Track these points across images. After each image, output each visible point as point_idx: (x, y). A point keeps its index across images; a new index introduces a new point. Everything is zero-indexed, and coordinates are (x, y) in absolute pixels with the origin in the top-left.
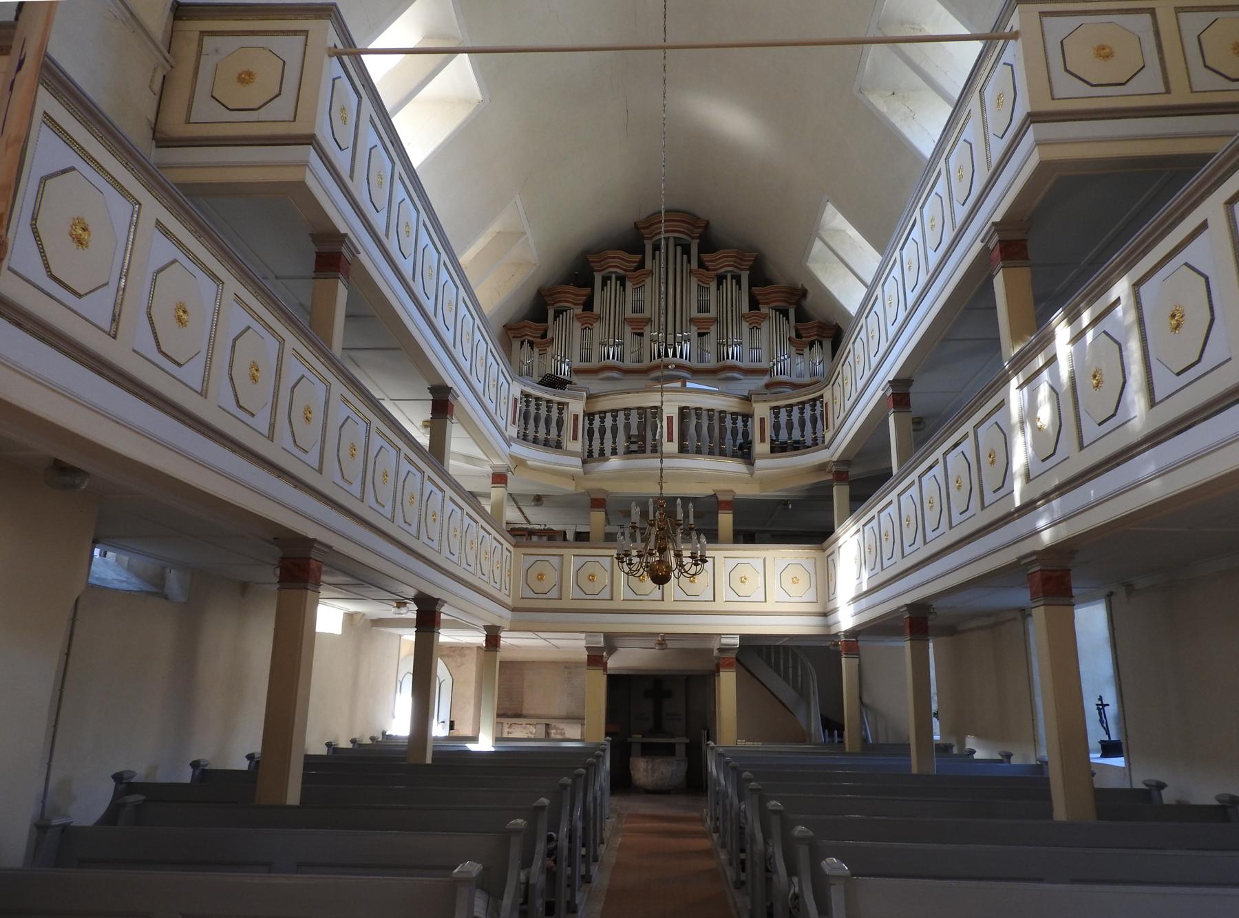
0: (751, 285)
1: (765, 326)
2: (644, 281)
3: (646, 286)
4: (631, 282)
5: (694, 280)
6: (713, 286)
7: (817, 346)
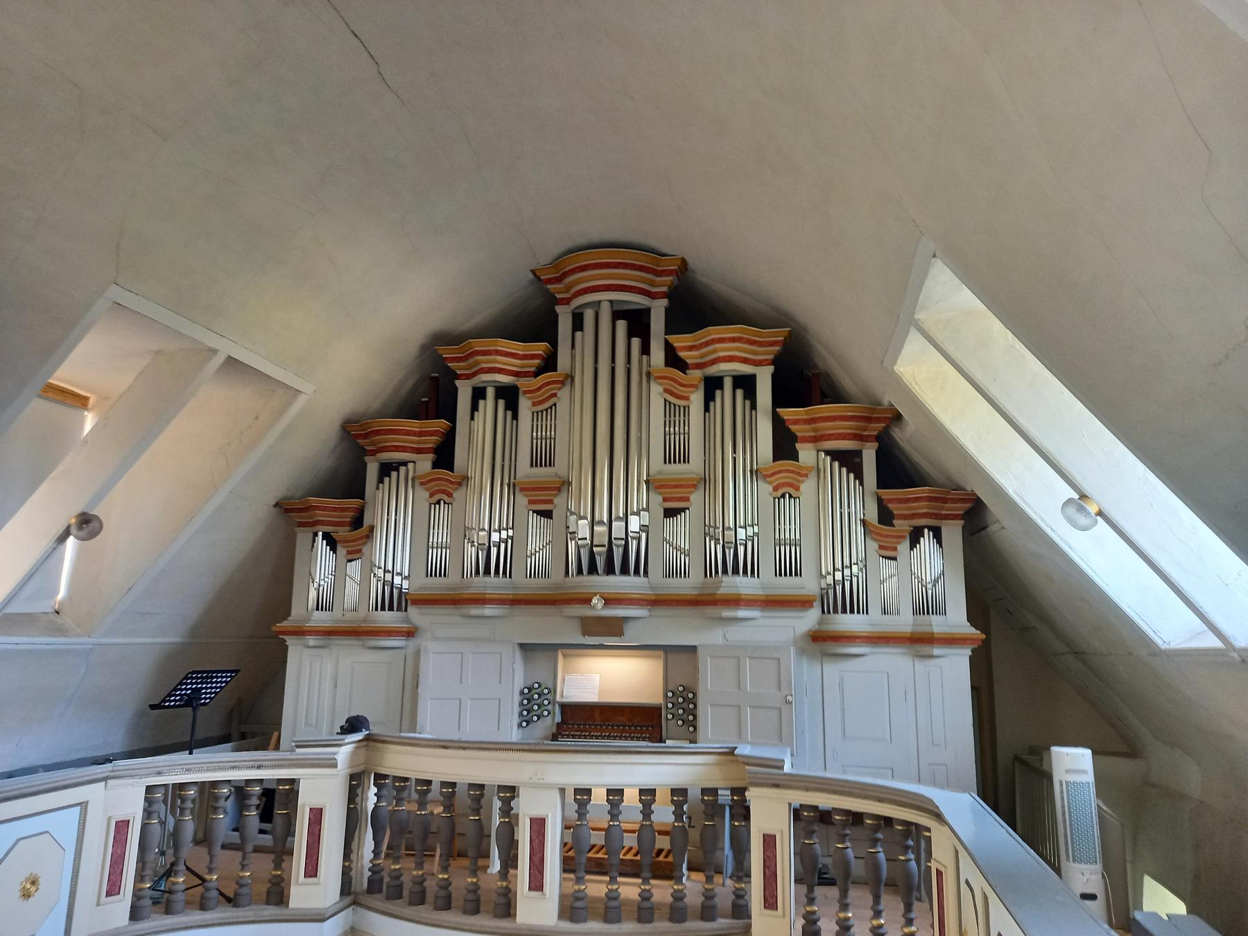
0: (780, 399)
1: (807, 487)
2: (555, 395)
3: (557, 405)
4: (529, 398)
5: (656, 389)
6: (696, 399)
7: (927, 542)
